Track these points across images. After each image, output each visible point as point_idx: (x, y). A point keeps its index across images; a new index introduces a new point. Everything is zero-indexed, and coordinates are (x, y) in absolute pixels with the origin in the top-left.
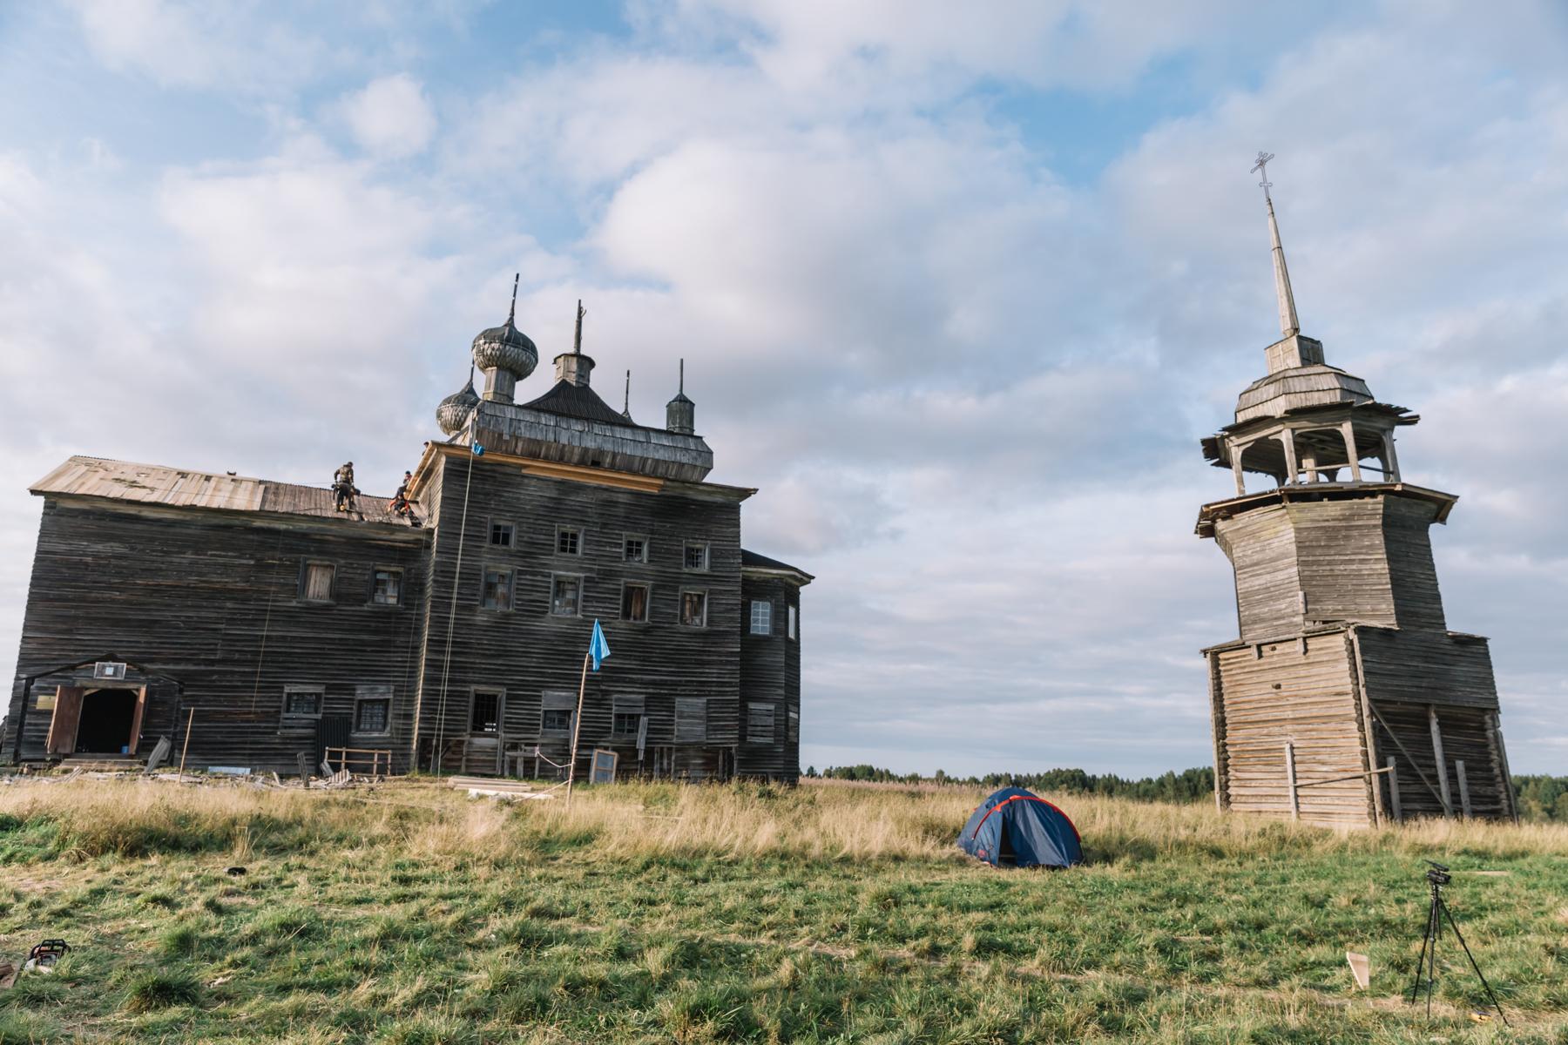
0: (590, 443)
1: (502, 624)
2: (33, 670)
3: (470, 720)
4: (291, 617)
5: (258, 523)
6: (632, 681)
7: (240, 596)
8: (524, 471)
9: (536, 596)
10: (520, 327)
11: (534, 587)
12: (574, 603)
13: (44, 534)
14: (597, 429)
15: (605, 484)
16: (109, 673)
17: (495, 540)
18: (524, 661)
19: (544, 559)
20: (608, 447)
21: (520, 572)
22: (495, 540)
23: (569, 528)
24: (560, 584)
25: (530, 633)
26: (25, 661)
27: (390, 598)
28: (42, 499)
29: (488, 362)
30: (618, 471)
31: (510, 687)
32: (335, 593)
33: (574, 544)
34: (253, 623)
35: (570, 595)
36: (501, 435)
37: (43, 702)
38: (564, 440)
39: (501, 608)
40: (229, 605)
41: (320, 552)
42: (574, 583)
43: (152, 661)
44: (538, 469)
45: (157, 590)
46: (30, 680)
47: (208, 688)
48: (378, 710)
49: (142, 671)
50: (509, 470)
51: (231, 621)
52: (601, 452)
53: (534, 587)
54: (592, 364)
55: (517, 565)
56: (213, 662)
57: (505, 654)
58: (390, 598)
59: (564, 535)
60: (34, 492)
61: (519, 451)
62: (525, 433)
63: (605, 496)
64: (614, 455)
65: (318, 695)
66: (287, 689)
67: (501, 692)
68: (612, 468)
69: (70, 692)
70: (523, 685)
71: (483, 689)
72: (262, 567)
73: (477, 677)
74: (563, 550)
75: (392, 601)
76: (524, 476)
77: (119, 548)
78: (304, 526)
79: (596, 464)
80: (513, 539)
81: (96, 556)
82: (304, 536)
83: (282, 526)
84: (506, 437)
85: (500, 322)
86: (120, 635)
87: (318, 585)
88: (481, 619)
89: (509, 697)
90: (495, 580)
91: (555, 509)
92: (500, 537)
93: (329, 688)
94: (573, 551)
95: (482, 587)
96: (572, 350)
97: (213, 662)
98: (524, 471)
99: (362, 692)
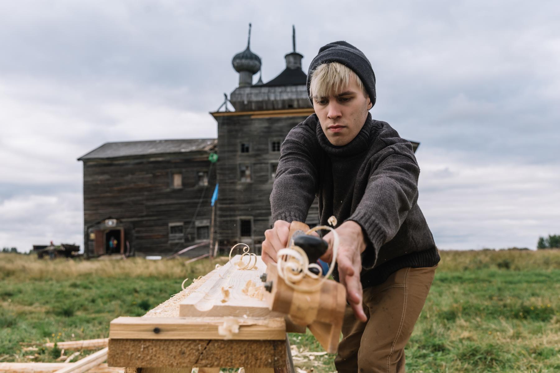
0: (285, 97)
1: (249, 188)
2: (89, 225)
3: (239, 232)
4: (168, 196)
5: (152, 159)
7: (149, 189)
8: (253, 117)
9: (263, 174)
10: (254, 50)
11: (261, 170)
13: (85, 175)
14: (289, 89)
15: (290, 116)
16: (111, 223)
17: (243, 151)
18: (259, 204)
20: (294, 97)
21: (255, 164)
22: (243, 151)
23: (275, 139)
25: (261, 191)
26: (86, 222)
27: (205, 183)
28: (81, 163)
29: (238, 68)
30: (303, 108)
31: (255, 216)
32: (184, 184)
33: (279, 147)
36: (243, 102)
37: (92, 236)
38: (272, 98)
39: (248, 180)
40: (146, 193)
43: (123, 218)
44: (258, 115)
45: (121, 191)
46: (88, 228)
48: (206, 231)
49: (121, 222)
50: (245, 118)
51: (147, 200)
52: (291, 100)
53: (261, 170)
54: (301, 57)
55: (253, 160)
56: (142, 217)
58: (205, 183)
59: (274, 143)
60: (79, 160)
61: (253, 107)
62: (254, 99)
63: (291, 121)
64: (298, 100)
65: (181, 226)
66: (171, 225)
67: (251, 218)
68: (299, 107)
69: (98, 232)
70: (260, 215)
71: (243, 218)
72: (155, 177)
73: (240, 213)
74: (274, 150)
75: (206, 184)
76: (252, 120)
77: (106, 177)
78: (168, 158)
79: (291, 107)
80: (250, 149)
81: (101, 181)
82: (168, 162)
83: (160, 159)
84: (246, 102)
85: (241, 49)
86: (111, 209)
87: (177, 181)
89: (255, 221)
90: (244, 168)
91: (268, 132)
92: (245, 149)
93: (186, 223)
94: (279, 150)
96: (291, 50)
97: (142, 217)
98: (253, 117)
99: (198, 224)
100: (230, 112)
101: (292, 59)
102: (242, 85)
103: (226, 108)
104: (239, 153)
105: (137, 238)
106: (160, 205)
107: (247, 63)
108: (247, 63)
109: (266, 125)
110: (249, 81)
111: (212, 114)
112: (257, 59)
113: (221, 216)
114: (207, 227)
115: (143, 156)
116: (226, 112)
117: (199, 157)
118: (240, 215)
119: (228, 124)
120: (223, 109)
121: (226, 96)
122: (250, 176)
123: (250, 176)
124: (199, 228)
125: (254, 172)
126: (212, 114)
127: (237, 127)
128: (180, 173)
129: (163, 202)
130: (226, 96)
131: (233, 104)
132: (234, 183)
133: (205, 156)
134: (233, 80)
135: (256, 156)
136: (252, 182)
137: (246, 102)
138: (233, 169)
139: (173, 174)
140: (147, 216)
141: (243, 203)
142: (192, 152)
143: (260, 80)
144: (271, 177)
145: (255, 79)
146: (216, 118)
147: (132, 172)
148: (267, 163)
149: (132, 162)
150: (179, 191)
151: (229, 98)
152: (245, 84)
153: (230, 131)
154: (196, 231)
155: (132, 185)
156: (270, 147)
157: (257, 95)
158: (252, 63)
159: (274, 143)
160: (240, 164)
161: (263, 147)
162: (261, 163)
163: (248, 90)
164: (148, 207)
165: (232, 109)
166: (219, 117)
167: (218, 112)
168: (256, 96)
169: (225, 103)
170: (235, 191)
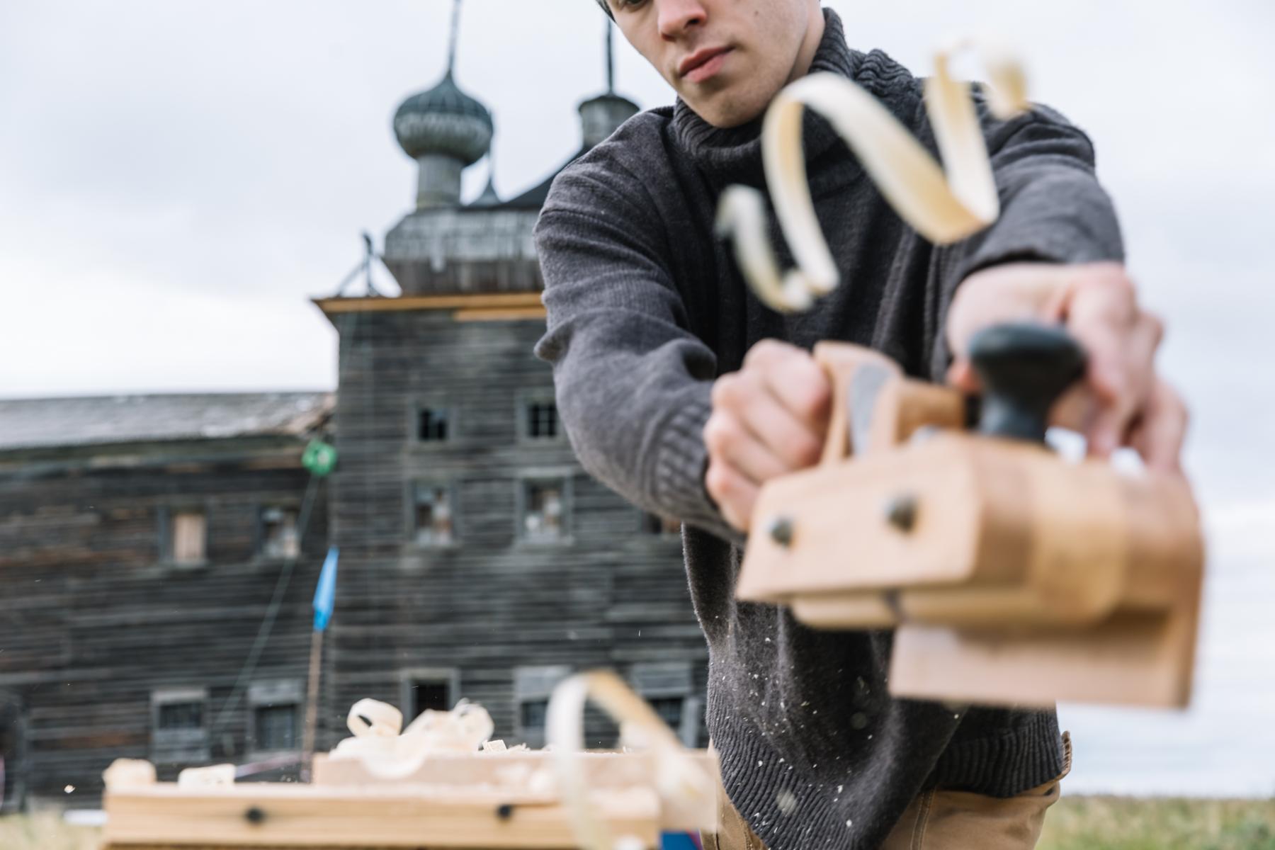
1: (444, 567)
4: (152, 592)
5: (100, 462)
6: (666, 642)
7: (85, 569)
8: (462, 316)
9: (495, 516)
10: (470, 84)
11: (489, 503)
12: (559, 520)
18: (481, 625)
19: (504, 454)
21: (467, 482)
24: (535, 493)
25: (489, 577)
27: (287, 546)
29: (415, 146)
31: (465, 667)
32: (212, 551)
34: (103, 606)
35: (553, 507)
39: (443, 540)
40: (73, 583)
41: (184, 490)
42: (556, 485)
47: (56, 702)
48: (287, 718)
51: (78, 607)
53: (489, 503)
55: (460, 469)
56: (57, 667)
57: (448, 615)
58: (287, 546)
59: (535, 410)
62: (468, 251)
65: (198, 704)
70: (485, 663)
71: (424, 673)
72: (109, 523)
74: (535, 432)
78: (156, 458)
80: (452, 429)
82: (157, 472)
83: (128, 461)
84: (438, 264)
85: (425, 79)
87: (188, 542)
88: (409, 563)
90: (427, 497)
92: (432, 429)
95: (408, 511)
96: (597, 87)
97: (57, 667)
98: (462, 316)
99: (259, 694)
100: (380, 297)
101: (600, 116)
102: (425, 204)
103: (370, 285)
104: (413, 442)
105: (37, 745)
106: (124, 627)
107: (444, 131)
108: (444, 131)
109: (507, 343)
110: (449, 188)
111: (319, 303)
112: (479, 112)
113: (343, 667)
114: (291, 708)
115: (65, 451)
116: (367, 298)
117: (268, 457)
118: (413, 664)
119: (376, 340)
120: (357, 288)
121: (368, 241)
122: (451, 525)
123: (451, 525)
124: (264, 711)
125: (466, 509)
126: (319, 303)
127: (406, 351)
128: (198, 510)
129: (136, 614)
130: (368, 241)
131: (395, 267)
132: (390, 550)
133: (290, 451)
134: (397, 182)
135: (471, 452)
136: (458, 544)
137: (438, 264)
138: (389, 498)
139: (172, 514)
140: (75, 664)
141: (421, 621)
142: (243, 439)
143: (490, 189)
144: (524, 529)
145: (472, 184)
146: (332, 317)
147: (26, 506)
148: (510, 480)
149: (28, 469)
150: (195, 575)
151: (379, 246)
152: (438, 200)
153: (380, 365)
154: (250, 720)
155: (24, 555)
156: (521, 421)
157: (477, 238)
158: (460, 126)
159: (535, 410)
160: (415, 484)
161: (496, 420)
162: (488, 480)
163: (446, 222)
164: (80, 634)
165: (388, 286)
166: (345, 314)
167: (338, 298)
168: (477, 243)
169: (365, 266)
170: (393, 576)
